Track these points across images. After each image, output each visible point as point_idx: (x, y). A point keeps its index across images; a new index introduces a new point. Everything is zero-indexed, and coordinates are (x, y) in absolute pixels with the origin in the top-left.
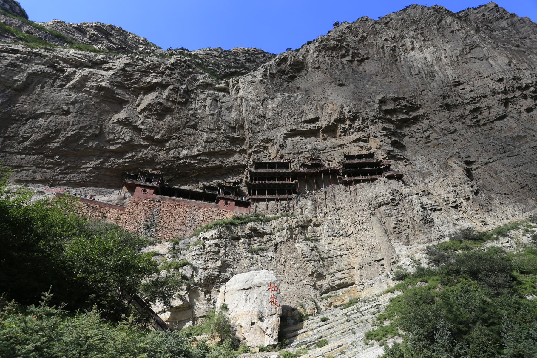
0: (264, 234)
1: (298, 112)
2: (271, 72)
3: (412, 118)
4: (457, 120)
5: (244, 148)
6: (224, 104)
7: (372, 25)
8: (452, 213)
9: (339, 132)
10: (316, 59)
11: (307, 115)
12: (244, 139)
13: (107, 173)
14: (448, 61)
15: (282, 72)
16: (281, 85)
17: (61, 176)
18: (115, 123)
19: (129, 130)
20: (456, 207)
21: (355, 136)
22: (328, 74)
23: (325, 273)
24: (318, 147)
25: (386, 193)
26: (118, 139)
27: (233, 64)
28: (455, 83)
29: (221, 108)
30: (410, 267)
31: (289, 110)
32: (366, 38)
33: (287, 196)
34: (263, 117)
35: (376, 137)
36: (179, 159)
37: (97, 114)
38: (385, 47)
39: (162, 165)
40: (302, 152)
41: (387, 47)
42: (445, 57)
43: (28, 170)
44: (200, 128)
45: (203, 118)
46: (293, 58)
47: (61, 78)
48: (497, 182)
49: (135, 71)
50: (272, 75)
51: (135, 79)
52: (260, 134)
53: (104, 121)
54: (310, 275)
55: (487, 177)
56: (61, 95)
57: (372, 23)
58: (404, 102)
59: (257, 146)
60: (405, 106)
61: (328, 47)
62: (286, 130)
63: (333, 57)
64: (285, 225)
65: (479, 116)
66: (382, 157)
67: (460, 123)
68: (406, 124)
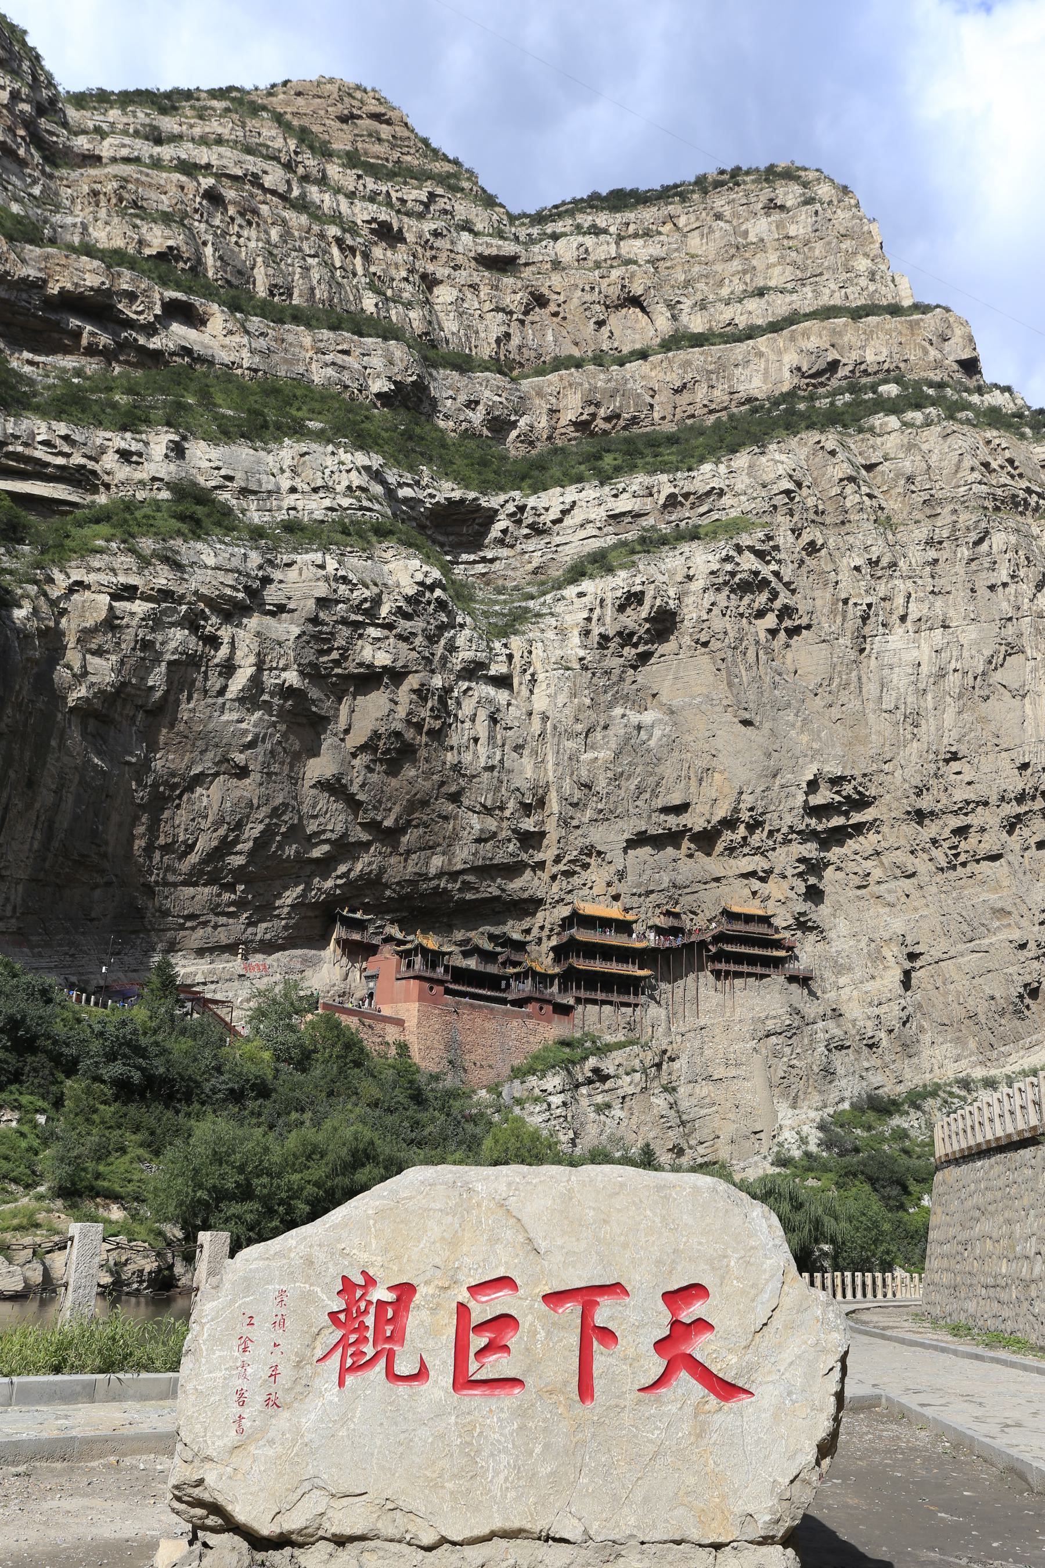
0: (607, 1077)
1: (652, 780)
2: (602, 630)
3: (852, 826)
4: (923, 850)
5: (539, 857)
6: (510, 733)
7: (841, 480)
8: (863, 1056)
9: (720, 847)
10: (705, 617)
11: (668, 791)
12: (542, 834)
13: (310, 914)
14: (958, 684)
15: (626, 638)
16: (621, 679)
17: (250, 930)
18: (313, 786)
19: (340, 806)
20: (870, 1046)
21: (746, 864)
22: (723, 672)
23: (685, 1146)
24: (680, 879)
25: (781, 1011)
26: (324, 831)
27: (335, 251)
28: (949, 756)
29: (503, 745)
30: (795, 1147)
31: (638, 770)
32: (819, 550)
33: (631, 999)
34: (588, 786)
35: (785, 877)
36: (426, 878)
37: (286, 768)
38: (851, 602)
39: (394, 891)
40: (652, 892)
41: (855, 604)
42: (955, 670)
43: (205, 924)
44: (466, 802)
45: (474, 776)
46: (658, 602)
47: (217, 665)
48: (941, 999)
49: (336, 622)
50: (604, 638)
51: (338, 649)
52: (579, 832)
53: (296, 784)
54: (669, 1150)
55: (930, 987)
56: (228, 722)
57: (841, 475)
58: (848, 789)
59: (570, 861)
60: (848, 797)
61: (737, 579)
62: (630, 827)
63: (742, 615)
64: (637, 1065)
65: (963, 843)
66: (785, 924)
67: (926, 856)
68: (838, 837)
